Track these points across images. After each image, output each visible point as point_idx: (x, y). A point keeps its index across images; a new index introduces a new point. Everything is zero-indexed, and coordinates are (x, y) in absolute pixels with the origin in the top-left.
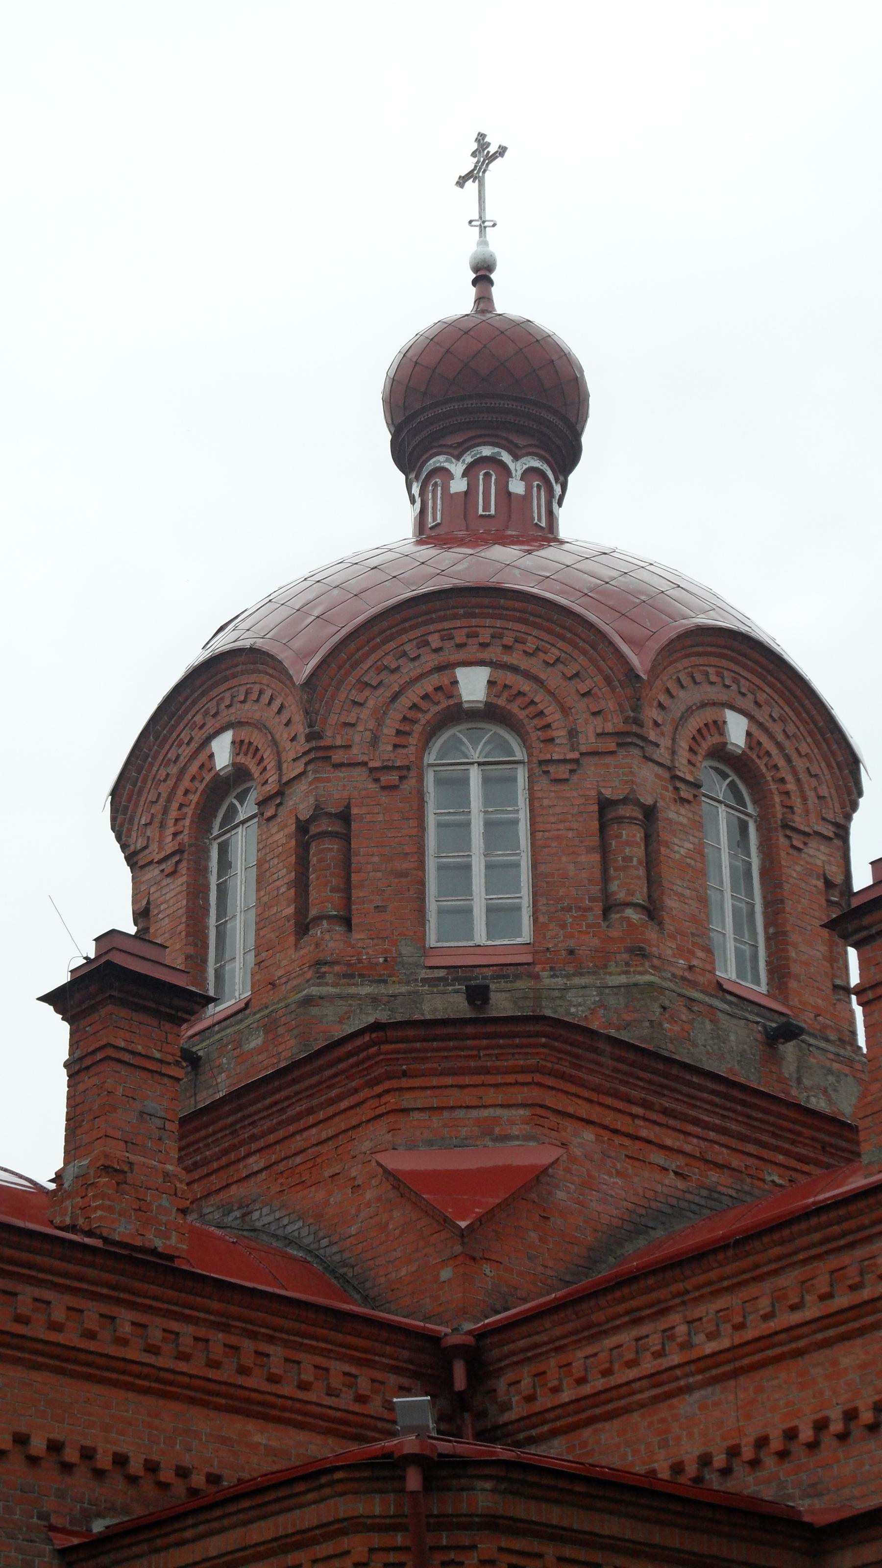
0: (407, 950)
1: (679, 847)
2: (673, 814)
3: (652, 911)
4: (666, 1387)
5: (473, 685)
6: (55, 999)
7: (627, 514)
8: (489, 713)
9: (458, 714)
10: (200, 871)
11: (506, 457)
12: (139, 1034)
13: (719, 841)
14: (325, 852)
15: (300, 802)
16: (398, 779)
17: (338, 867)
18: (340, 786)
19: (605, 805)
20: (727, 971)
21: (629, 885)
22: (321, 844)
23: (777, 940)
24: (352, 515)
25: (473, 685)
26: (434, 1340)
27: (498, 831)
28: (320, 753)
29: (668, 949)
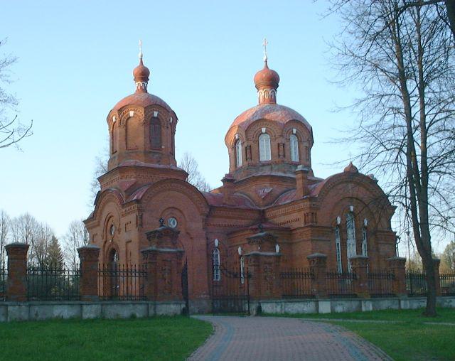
0: (258, 162)
1: (287, 148)
2: (287, 144)
3: (284, 156)
4: (280, 215)
5: (264, 130)
6: (222, 180)
7: (283, 98)
8: (266, 133)
9: (262, 133)
10: (235, 150)
11: (268, 90)
12: (230, 184)
13: (294, 146)
14: (248, 151)
15: (246, 145)
16: (257, 142)
17: (251, 152)
18: (251, 143)
19: (279, 144)
20: (293, 160)
21: (281, 153)
22: (248, 150)
23: (300, 155)
24: (250, 100)
25: (264, 130)
26: (259, 210)
27: (267, 146)
28: (247, 140)
29: (285, 160)
